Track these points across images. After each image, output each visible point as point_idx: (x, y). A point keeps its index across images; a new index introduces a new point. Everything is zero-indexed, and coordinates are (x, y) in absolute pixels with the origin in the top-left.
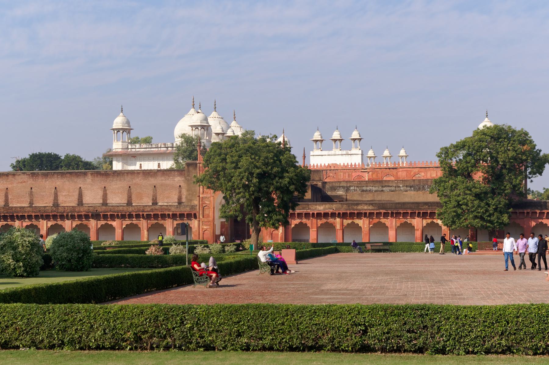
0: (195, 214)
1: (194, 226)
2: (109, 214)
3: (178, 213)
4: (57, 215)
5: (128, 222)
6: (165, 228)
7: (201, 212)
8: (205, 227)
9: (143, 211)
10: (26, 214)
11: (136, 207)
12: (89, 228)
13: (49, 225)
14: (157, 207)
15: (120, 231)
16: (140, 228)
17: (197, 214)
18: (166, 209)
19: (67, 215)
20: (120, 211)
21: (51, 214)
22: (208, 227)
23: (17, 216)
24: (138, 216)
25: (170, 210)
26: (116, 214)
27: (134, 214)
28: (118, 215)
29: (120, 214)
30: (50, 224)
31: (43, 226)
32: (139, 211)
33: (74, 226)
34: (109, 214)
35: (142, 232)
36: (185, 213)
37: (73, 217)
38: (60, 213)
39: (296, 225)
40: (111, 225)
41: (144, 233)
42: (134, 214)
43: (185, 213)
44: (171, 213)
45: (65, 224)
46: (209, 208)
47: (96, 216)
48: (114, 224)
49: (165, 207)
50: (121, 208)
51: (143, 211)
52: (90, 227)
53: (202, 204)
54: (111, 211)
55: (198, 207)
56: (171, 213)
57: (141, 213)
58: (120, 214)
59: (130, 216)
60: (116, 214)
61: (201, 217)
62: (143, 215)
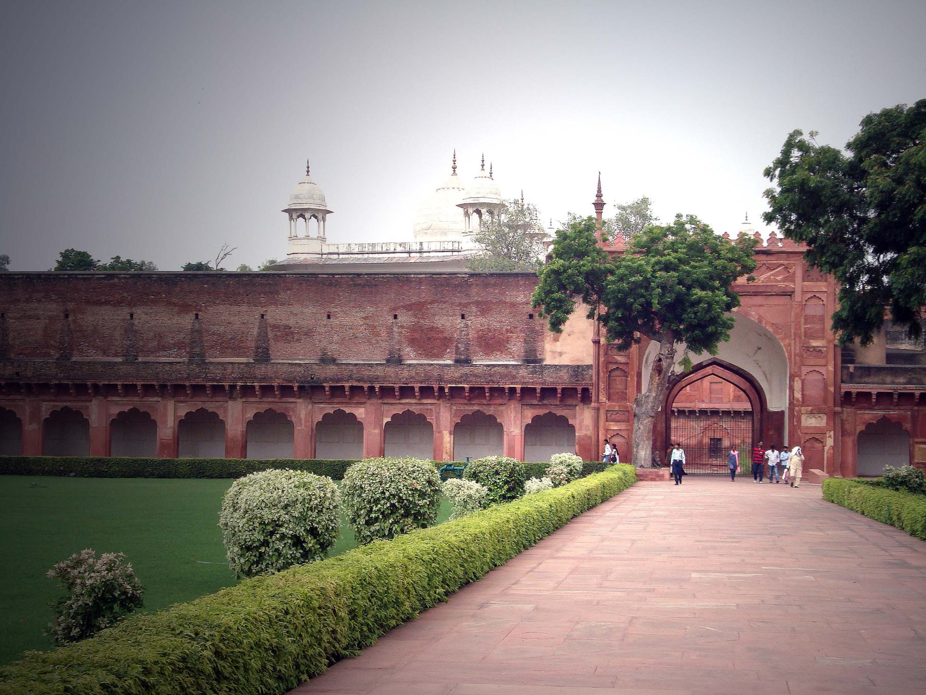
0: (586, 391)
1: (581, 422)
2: (347, 385)
3: (538, 387)
4: (204, 386)
5: (398, 408)
6: (500, 426)
7: (602, 386)
8: (614, 427)
9: (440, 379)
10: (119, 383)
11: (421, 370)
12: (291, 423)
13: (182, 413)
14: (466, 370)
15: (377, 431)
16: (430, 424)
17: (593, 392)
18: (503, 376)
19: (233, 387)
20: (377, 378)
21: (187, 384)
22: (623, 426)
23: (95, 386)
24: (426, 392)
25: (514, 377)
26: (366, 386)
27: (417, 386)
28: (372, 389)
29: (377, 386)
30: (183, 410)
31: (165, 415)
32: (428, 378)
33: (250, 415)
34: (347, 385)
35: (436, 435)
36: (559, 387)
37: (247, 391)
38: (214, 380)
39: (869, 426)
40: (352, 416)
41: (442, 438)
42: (417, 386)
43: (559, 387)
44: (519, 386)
45: (226, 410)
46: (625, 374)
47: (311, 389)
48: (360, 412)
49: (501, 370)
50: (379, 372)
51: (440, 379)
52: (294, 419)
53: (608, 363)
54: (350, 378)
55: (593, 372)
56: (519, 386)
57: (436, 386)
58: (377, 386)
59: (406, 391)
60: (366, 386)
61: (603, 398)
62: (441, 389)
